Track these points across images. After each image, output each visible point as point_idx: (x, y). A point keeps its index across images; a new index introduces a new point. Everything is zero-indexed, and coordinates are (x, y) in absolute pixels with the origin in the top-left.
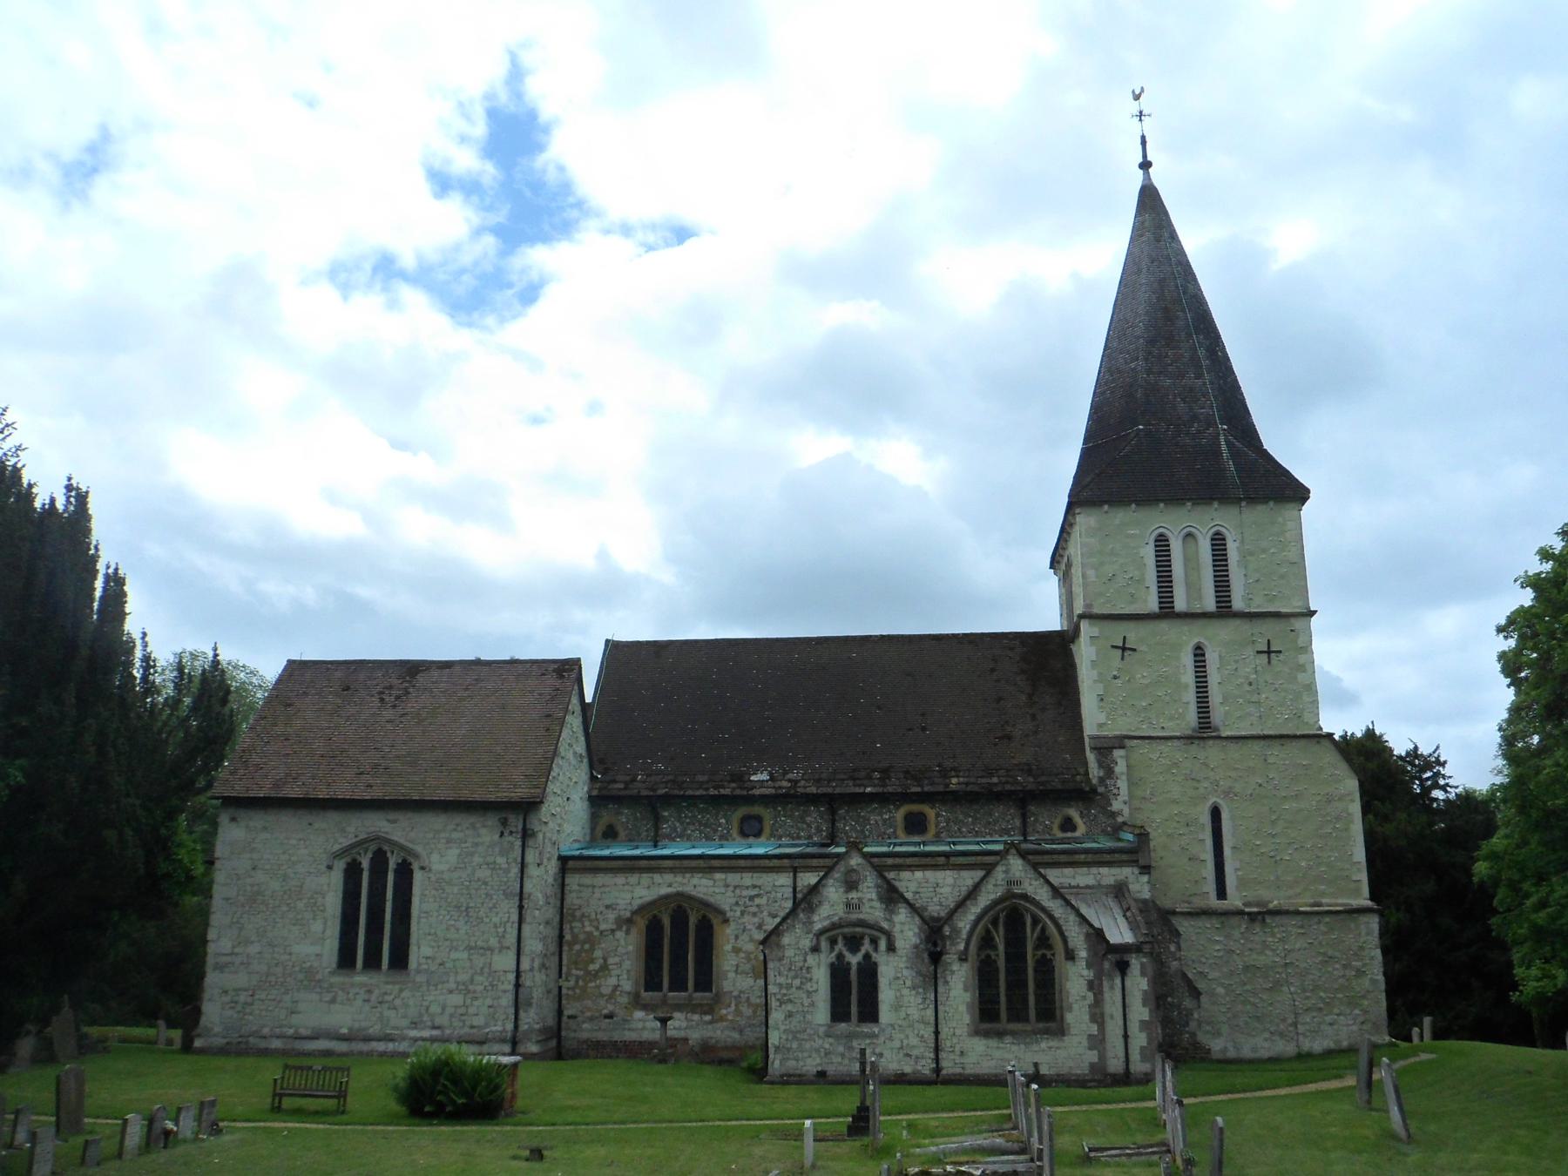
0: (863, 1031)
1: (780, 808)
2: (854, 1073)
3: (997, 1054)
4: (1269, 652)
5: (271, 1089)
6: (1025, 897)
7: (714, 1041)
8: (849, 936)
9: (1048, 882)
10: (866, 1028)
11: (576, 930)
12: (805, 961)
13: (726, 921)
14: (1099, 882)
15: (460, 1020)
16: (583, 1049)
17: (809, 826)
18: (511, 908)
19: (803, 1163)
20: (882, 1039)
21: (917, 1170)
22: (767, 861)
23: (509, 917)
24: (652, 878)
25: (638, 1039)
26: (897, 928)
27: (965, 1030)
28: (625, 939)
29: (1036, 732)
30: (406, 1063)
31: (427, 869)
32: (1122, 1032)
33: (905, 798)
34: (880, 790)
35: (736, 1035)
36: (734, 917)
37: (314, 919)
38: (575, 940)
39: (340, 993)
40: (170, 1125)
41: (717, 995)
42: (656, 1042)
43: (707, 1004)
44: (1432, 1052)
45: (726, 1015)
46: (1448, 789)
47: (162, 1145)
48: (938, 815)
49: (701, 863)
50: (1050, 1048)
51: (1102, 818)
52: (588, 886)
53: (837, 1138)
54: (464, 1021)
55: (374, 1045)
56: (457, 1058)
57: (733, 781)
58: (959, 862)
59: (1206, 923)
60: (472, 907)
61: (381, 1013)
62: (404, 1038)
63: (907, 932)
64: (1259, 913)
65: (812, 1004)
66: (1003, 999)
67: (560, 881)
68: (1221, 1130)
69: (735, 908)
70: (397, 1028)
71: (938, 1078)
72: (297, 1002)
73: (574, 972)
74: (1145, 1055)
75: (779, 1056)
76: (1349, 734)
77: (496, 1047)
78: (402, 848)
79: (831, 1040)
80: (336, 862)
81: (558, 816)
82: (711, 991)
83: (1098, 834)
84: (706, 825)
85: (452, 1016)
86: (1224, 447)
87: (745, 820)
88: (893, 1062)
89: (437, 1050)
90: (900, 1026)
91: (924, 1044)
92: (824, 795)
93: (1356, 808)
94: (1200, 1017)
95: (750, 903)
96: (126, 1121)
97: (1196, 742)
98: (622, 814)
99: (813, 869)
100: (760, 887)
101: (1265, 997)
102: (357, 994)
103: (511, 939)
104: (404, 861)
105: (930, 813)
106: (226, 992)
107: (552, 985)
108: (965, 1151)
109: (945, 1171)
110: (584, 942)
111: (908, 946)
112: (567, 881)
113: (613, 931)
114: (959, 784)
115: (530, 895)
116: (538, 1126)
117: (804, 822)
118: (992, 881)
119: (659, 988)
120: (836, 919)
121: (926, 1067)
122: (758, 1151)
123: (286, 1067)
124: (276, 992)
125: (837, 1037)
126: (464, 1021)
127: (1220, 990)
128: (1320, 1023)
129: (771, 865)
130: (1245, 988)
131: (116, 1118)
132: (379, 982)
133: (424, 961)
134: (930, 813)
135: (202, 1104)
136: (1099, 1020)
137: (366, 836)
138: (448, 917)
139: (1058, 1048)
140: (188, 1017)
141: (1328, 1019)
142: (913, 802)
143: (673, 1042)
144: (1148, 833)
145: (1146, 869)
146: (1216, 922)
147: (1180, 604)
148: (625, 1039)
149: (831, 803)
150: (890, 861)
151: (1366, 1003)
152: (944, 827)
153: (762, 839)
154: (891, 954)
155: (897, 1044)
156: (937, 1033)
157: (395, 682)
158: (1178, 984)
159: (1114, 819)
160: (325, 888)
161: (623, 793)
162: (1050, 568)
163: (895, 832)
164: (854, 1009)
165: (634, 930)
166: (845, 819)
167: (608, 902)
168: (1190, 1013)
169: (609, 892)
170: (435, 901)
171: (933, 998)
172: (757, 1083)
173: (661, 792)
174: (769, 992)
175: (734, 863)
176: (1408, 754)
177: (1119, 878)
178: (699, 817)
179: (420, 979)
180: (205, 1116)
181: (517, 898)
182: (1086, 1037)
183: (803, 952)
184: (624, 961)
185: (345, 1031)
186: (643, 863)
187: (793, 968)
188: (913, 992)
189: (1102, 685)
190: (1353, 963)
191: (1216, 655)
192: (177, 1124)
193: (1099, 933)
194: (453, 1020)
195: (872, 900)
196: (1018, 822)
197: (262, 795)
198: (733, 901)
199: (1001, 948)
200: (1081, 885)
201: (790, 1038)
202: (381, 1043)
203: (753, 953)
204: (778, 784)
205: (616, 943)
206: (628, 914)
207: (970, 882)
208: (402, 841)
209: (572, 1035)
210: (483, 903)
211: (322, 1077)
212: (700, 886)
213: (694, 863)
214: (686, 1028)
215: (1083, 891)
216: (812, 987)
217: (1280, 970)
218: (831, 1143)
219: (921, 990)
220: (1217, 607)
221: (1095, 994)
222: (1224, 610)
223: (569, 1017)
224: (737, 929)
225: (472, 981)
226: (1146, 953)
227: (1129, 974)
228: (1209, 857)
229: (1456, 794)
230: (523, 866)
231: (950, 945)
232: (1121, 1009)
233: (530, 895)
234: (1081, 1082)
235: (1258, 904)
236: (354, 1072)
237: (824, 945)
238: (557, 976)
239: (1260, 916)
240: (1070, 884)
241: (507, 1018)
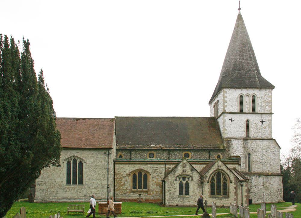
11: (117, 176)
12: (174, 182)
17: (164, 156)
26: (194, 176)
33: (185, 150)
38: (118, 178)
39: (68, 189)
48: (191, 154)
49: (145, 162)
50: (226, 200)
51: (226, 155)
52: (120, 167)
55: (76, 200)
61: (77, 194)
63: (196, 177)
65: (175, 191)
73: (117, 185)
78: (80, 158)
79: (179, 198)
87: (150, 154)
92: (167, 149)
103: (106, 178)
105: (190, 153)
106: (41, 190)
110: (119, 179)
112: (115, 166)
113: (126, 176)
117: (163, 155)
120: (180, 174)
132: (77, 187)
142: (186, 151)
153: (154, 158)
155: (193, 199)
164: (184, 192)
167: (125, 171)
171: (201, 190)
175: (152, 162)
177: (235, 167)
179: (86, 186)
196: (208, 156)
198: (152, 170)
199: (216, 180)
206: (129, 173)
213: (143, 162)
225: (98, 186)
230: (108, 162)
232: (241, 193)
237: (178, 179)
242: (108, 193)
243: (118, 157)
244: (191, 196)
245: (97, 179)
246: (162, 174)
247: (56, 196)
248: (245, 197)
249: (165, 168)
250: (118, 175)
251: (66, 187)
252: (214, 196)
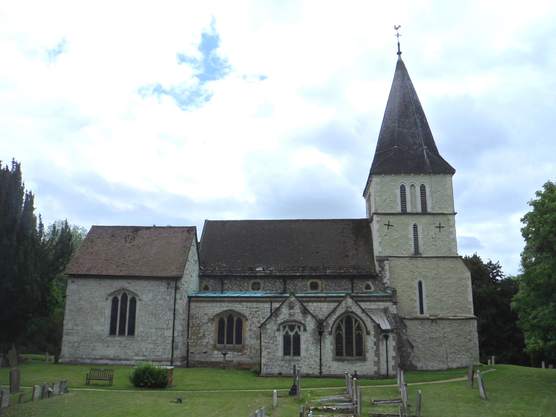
1: (266, 280)
2: (291, 373)
3: (342, 367)
4: (440, 227)
5: (86, 377)
6: (352, 312)
7: (242, 362)
8: (290, 325)
9: (361, 307)
10: (296, 358)
11: (194, 322)
12: (275, 334)
13: (247, 320)
14: (378, 307)
15: (153, 353)
16: (196, 364)
18: (171, 314)
19: (273, 405)
20: (301, 362)
21: (313, 408)
22: (261, 299)
23: (170, 318)
24: (221, 304)
25: (216, 361)
26: (307, 323)
28: (211, 325)
29: (357, 254)
30: (134, 368)
31: (141, 300)
32: (386, 360)
33: (311, 277)
34: (302, 274)
35: (250, 360)
36: (250, 318)
37: (101, 317)
38: (193, 326)
39: (110, 343)
40: (50, 389)
41: (243, 346)
42: (222, 362)
43: (240, 349)
44: (494, 369)
45: (246, 353)
46: (502, 276)
47: (47, 396)
48: (322, 283)
49: (238, 299)
50: (361, 365)
51: (380, 285)
52: (198, 307)
53: (285, 396)
54: (154, 354)
55: (122, 362)
56: (151, 367)
57: (250, 271)
58: (329, 300)
59: (416, 322)
60: (157, 314)
61: (125, 351)
62: (132, 360)
63: (311, 324)
64: (435, 319)
65: (277, 349)
66: (344, 348)
67: (188, 305)
68: (420, 395)
69: (250, 315)
70: (131, 356)
71: (321, 376)
72: (95, 346)
73: (193, 337)
74: (394, 368)
75: (265, 367)
76: (467, 256)
77: (166, 363)
79: (283, 362)
80: (109, 297)
81: (188, 282)
82: (241, 344)
83: (378, 290)
84: (240, 286)
85: (150, 352)
86: (425, 154)
87: (254, 284)
88: (305, 370)
89: (144, 364)
90: (308, 357)
91: (316, 364)
92: (282, 276)
93: (469, 283)
94: (413, 355)
95: (256, 314)
96: (34, 388)
97: (414, 259)
98: (210, 281)
99: (278, 302)
100: (259, 308)
101: (436, 348)
102: (116, 344)
103: (171, 326)
104: (133, 297)
105: (319, 282)
106: (70, 343)
107: (185, 342)
108: (330, 401)
109: (323, 408)
110: (196, 327)
111: (311, 329)
113: (207, 323)
114: (329, 272)
115: (177, 310)
116: (180, 391)
118: (341, 306)
119: (223, 343)
121: (317, 372)
122: (257, 400)
123: (91, 369)
124: (88, 343)
125: (286, 361)
126: (154, 354)
127: (421, 346)
128: (456, 358)
130: (430, 345)
131: (31, 387)
132: (124, 340)
133: (140, 333)
134: (319, 282)
135: (62, 382)
136: (378, 356)
137: (120, 288)
138: (148, 317)
139: (363, 365)
140: (57, 351)
141: (458, 356)
143: (228, 362)
144: (396, 290)
145: (395, 303)
146: (419, 322)
147: (409, 210)
148: (211, 361)
149: (285, 279)
150: (305, 299)
151: (472, 351)
152: (324, 288)
153: (260, 291)
154: (305, 332)
155: (307, 363)
156: (321, 360)
157: (131, 234)
158: (406, 343)
159: (384, 285)
160: (105, 306)
161: (210, 274)
162: (363, 196)
163: (307, 289)
164: (292, 351)
165: (214, 323)
166: (289, 284)
168: (410, 354)
169: (206, 309)
170: (144, 312)
172: (257, 377)
173: (224, 274)
174: (262, 345)
175: (249, 299)
176: (488, 264)
177: (386, 306)
178: (238, 283)
179: (139, 339)
180: (62, 387)
181: (173, 311)
182: (373, 362)
183: (274, 331)
184: (211, 333)
185: (112, 357)
186: (218, 299)
187: (270, 336)
188: (313, 345)
189: (380, 238)
190: (468, 337)
191: (421, 228)
192: (52, 389)
193: (378, 326)
194: (150, 353)
195: (298, 313)
196: (350, 286)
197: (83, 274)
198: (249, 313)
199: (344, 330)
200: (372, 308)
202: (125, 361)
203: (256, 331)
204: (266, 272)
205: (208, 327)
206: (212, 317)
207: (333, 307)
208: (132, 290)
209: (192, 359)
210: (161, 313)
211: (104, 373)
212: (238, 307)
213: (235, 299)
214: (232, 357)
215: (373, 310)
216: (277, 343)
217: (442, 339)
218: (283, 398)
219: (315, 345)
220: (422, 211)
221: (377, 347)
222: (424, 212)
223: (191, 353)
224: (251, 323)
225: (157, 340)
226: (395, 333)
227: (389, 340)
228: (417, 299)
229: (505, 278)
230: (175, 299)
231: (326, 329)
232: (386, 352)
233: (177, 310)
234: (371, 378)
235: (435, 316)
236: (115, 372)
237: (281, 328)
238: (187, 338)
239: (435, 320)
240: (368, 308)
241: (169, 353)
242: (173, 351)
243: (202, 288)
244: (304, 359)
245: (157, 327)
247: (91, 354)
248: (393, 359)
250: (195, 320)
251: (108, 339)
252: (342, 357)
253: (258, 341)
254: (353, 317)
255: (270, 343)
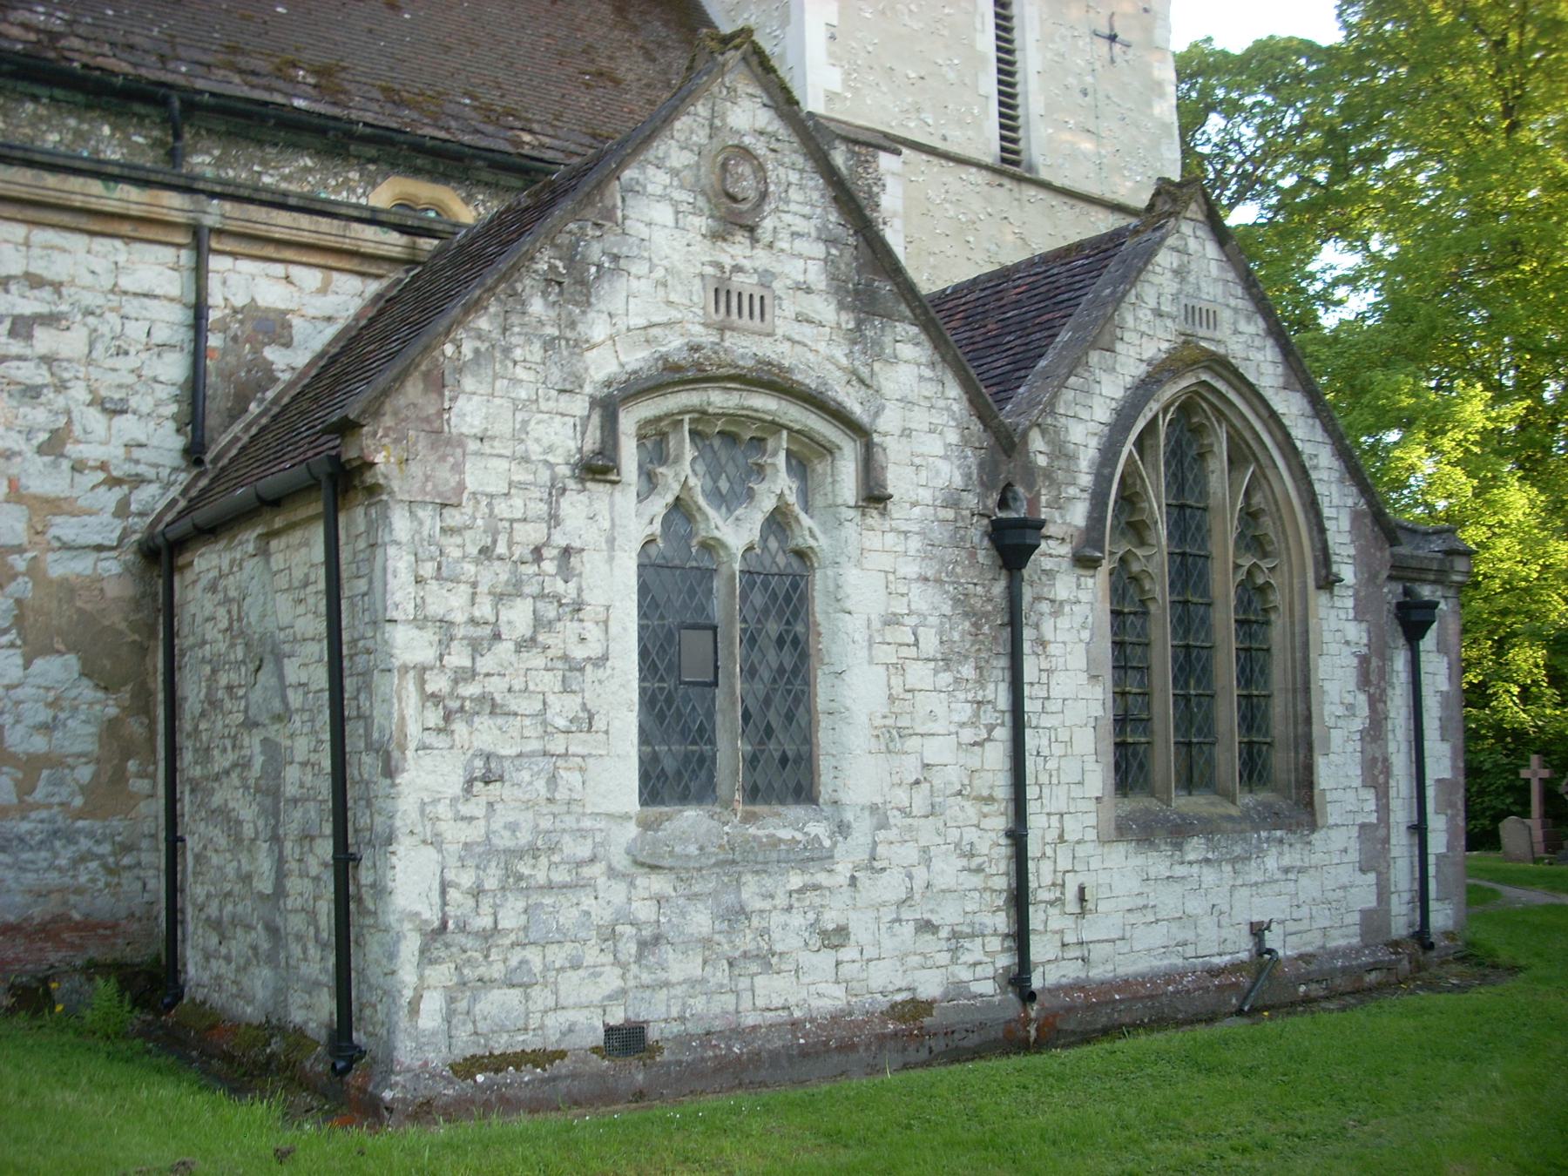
0: (776, 842)
6: (1222, 365)
12: (554, 519)
20: (843, 869)
22: (96, 187)
27: (1091, 820)
50: (1286, 870)
65: (586, 721)
79: (658, 884)
95: (16, 347)
99: (270, 251)
100: (57, 287)
111: (925, 495)
120: (673, 344)
125: (681, 871)
129: (111, 206)
154: (874, 518)
155: (889, 887)
156: (1017, 837)
171: (1003, 701)
182: (1355, 832)
183: (545, 476)
187: (501, 549)
188: (946, 678)
201: (491, 883)
203: (20, 550)
219: (968, 671)
246: (128, 427)
249: (199, 310)
253: (39, 664)
254: (1221, 415)
255: (497, 636)
